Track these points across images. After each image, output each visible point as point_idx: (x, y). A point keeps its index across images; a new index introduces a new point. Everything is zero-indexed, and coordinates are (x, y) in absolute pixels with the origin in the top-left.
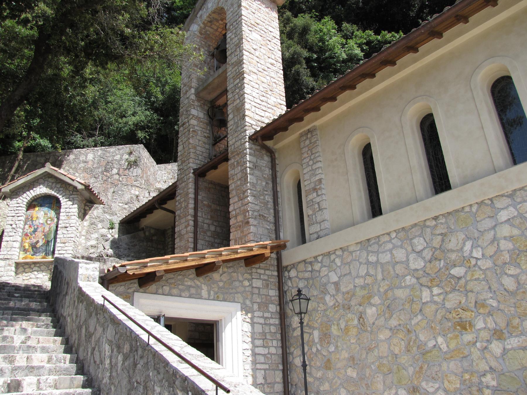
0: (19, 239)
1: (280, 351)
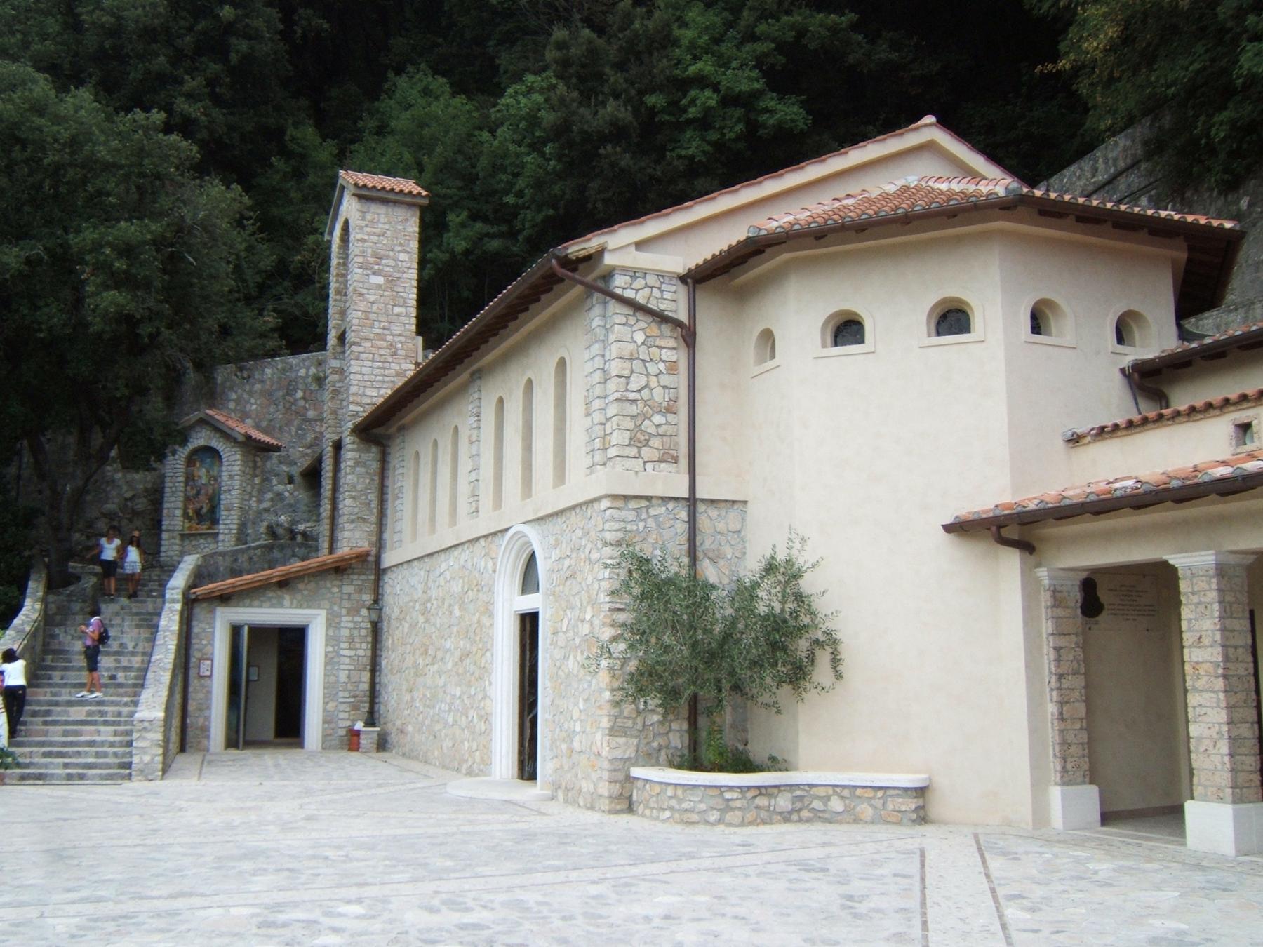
0: (181, 505)
1: (369, 653)
